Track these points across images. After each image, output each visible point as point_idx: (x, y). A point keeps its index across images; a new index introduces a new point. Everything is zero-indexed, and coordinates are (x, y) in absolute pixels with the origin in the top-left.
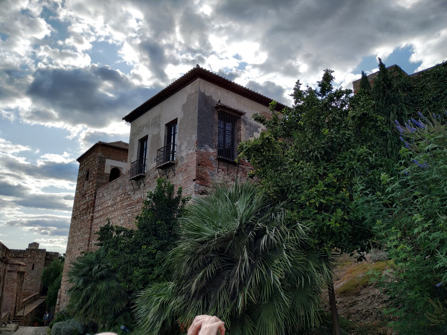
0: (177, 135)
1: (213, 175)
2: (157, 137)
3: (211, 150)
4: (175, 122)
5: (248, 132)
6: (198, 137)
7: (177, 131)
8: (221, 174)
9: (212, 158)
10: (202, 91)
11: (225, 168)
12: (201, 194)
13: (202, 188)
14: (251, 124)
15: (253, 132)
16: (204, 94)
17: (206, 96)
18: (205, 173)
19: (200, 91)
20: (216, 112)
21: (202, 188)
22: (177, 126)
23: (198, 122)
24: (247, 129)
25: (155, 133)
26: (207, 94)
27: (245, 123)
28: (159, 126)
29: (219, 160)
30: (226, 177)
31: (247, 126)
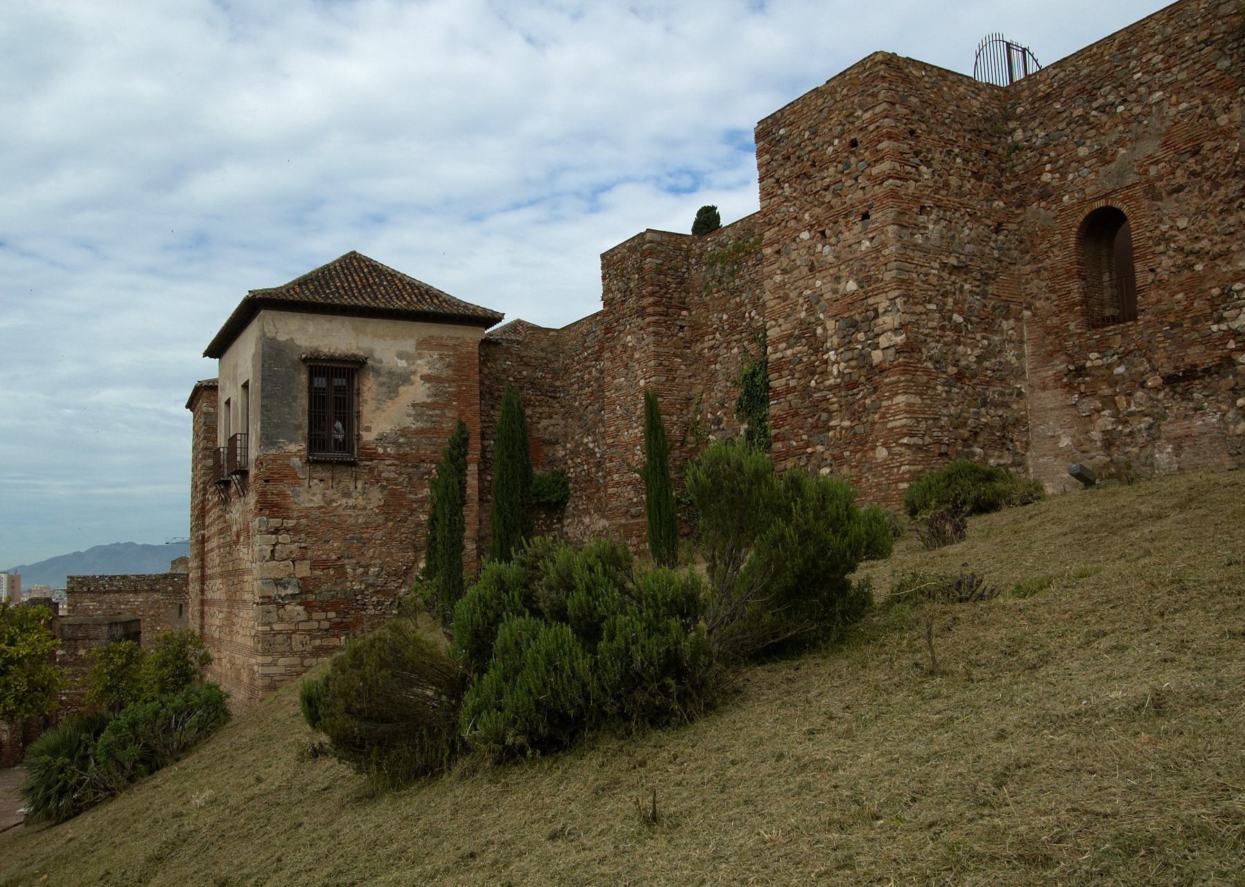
3: (293, 448)
5: (384, 389)
12: (273, 533)
13: (275, 522)
14: (391, 374)
15: (398, 386)
19: (264, 334)
21: (275, 522)
26: (282, 337)
27: (377, 372)
30: (329, 492)
31: (381, 379)
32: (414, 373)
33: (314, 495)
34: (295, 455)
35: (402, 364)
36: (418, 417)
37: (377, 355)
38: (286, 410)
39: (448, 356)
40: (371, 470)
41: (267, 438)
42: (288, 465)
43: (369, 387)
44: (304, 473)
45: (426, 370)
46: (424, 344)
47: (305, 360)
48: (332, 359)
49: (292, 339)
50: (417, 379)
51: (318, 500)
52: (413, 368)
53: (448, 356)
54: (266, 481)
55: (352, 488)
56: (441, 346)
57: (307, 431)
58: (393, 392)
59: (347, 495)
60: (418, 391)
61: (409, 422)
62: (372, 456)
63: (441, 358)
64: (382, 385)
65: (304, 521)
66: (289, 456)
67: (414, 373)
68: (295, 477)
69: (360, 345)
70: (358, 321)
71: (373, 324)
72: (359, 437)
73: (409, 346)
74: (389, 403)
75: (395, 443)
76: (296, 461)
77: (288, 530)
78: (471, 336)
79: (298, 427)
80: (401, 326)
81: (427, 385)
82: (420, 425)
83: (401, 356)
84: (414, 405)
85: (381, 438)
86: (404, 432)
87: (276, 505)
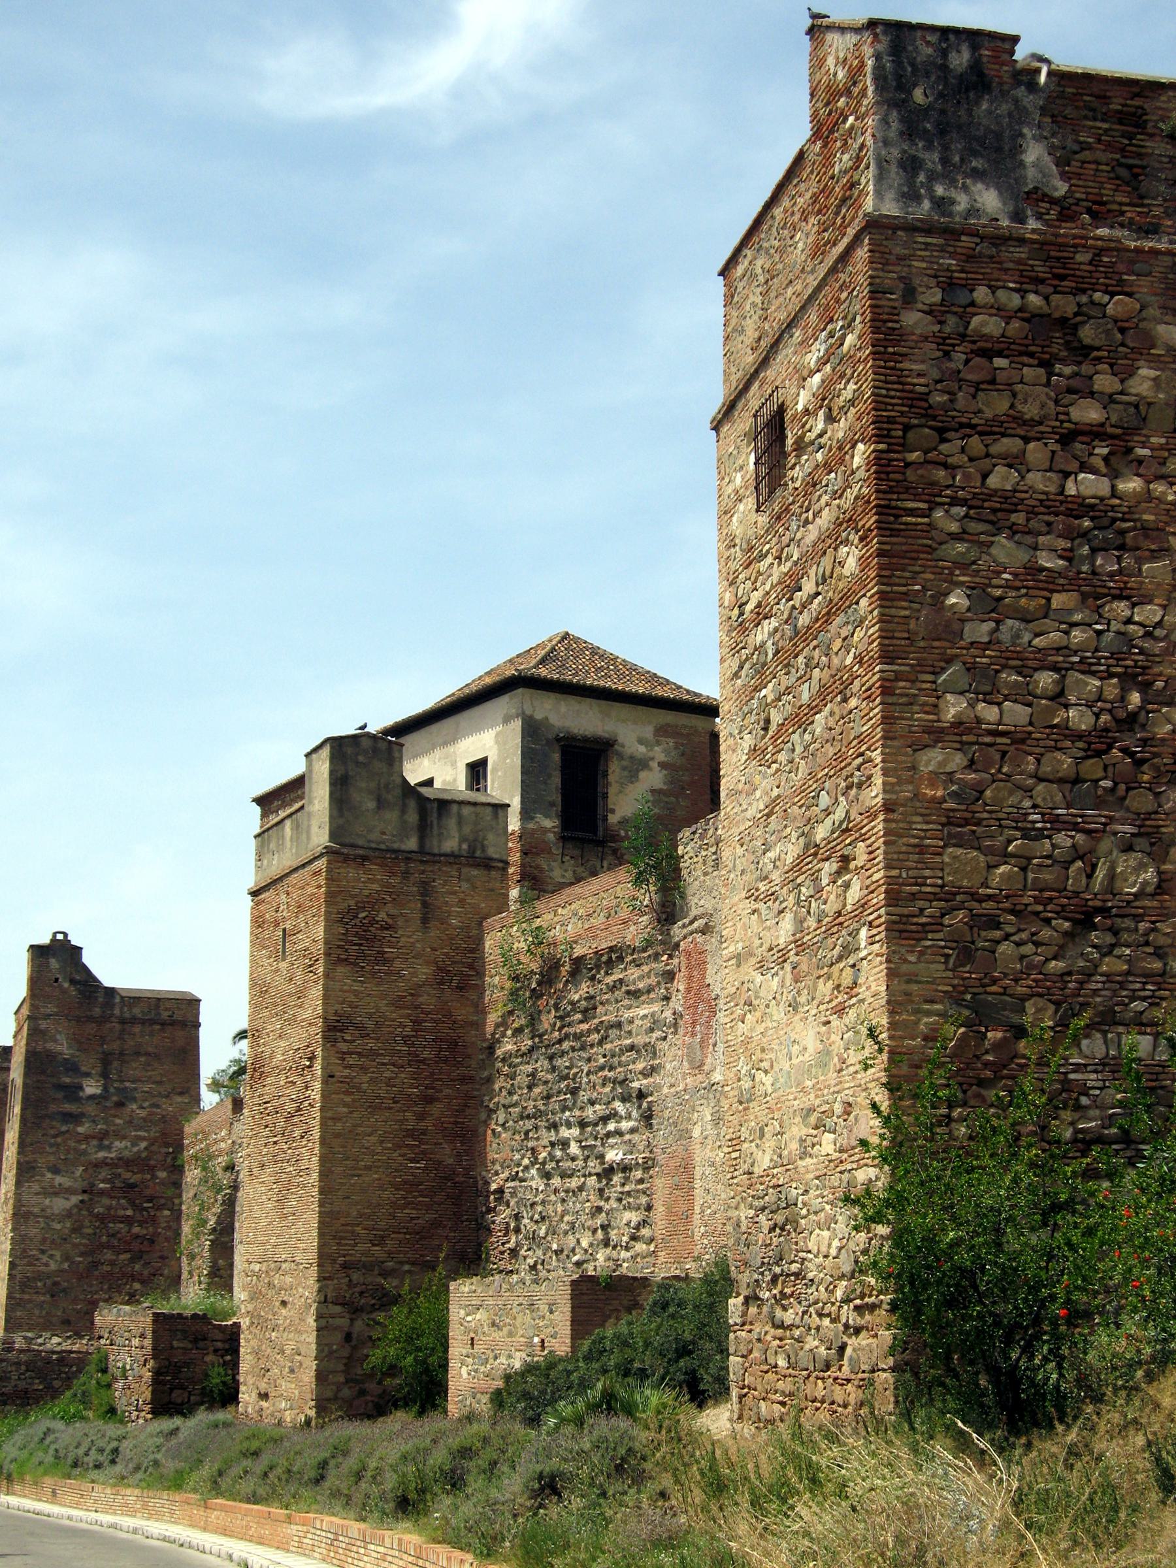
3: (548, 823)
4: (483, 762)
5: (626, 773)
6: (522, 802)
9: (551, 836)
10: (528, 712)
11: (577, 852)
14: (632, 757)
15: (638, 771)
16: (531, 717)
17: (536, 721)
18: (538, 867)
19: (523, 713)
20: (557, 748)
26: (539, 716)
27: (621, 756)
29: (564, 839)
31: (624, 763)
32: (652, 759)
33: (566, 871)
34: (549, 830)
35: (642, 749)
37: (621, 739)
38: (542, 787)
39: (682, 745)
41: (526, 812)
42: (544, 841)
43: (615, 770)
44: (558, 849)
45: (662, 757)
46: (662, 731)
47: (558, 739)
49: (547, 718)
50: (654, 764)
52: (651, 754)
53: (682, 745)
54: (525, 854)
55: (599, 867)
57: (560, 809)
60: (653, 778)
62: (615, 838)
64: (624, 768)
66: (545, 831)
67: (652, 759)
68: (550, 852)
69: (606, 728)
72: (605, 819)
73: (648, 732)
76: (551, 836)
79: (552, 804)
80: (641, 710)
81: (664, 772)
82: (656, 810)
83: (641, 741)
84: (653, 791)
85: (624, 822)
87: (534, 878)
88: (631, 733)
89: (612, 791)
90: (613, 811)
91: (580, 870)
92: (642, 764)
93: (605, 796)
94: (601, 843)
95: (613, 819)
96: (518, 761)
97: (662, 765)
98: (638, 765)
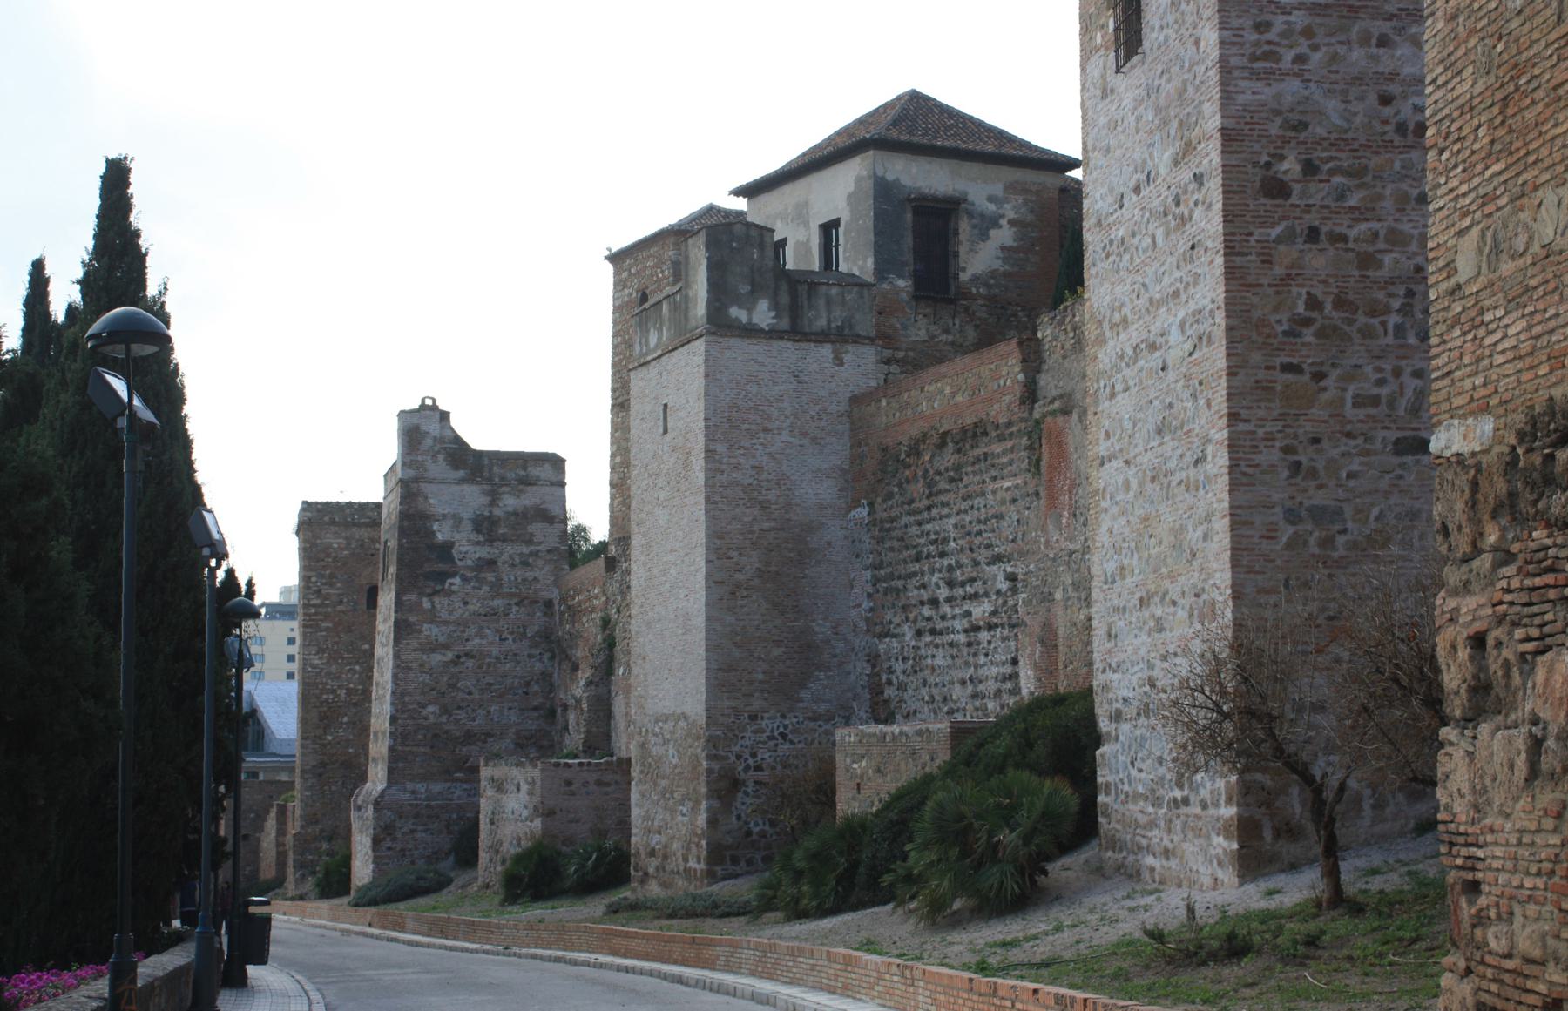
0: (841, 249)
1: (905, 328)
2: (804, 246)
3: (901, 283)
5: (976, 231)
6: (876, 263)
7: (841, 241)
8: (922, 322)
9: (904, 296)
10: (880, 174)
13: (887, 353)
14: (982, 216)
15: (988, 229)
16: (883, 178)
21: (887, 353)
22: (841, 230)
23: (876, 235)
24: (974, 227)
25: (802, 238)
26: (890, 177)
27: (971, 215)
28: (806, 224)
29: (916, 298)
31: (975, 221)
32: (1002, 216)
35: (992, 207)
36: (1005, 260)
37: (971, 198)
40: (967, 309)
45: (1011, 215)
46: (1011, 188)
48: (935, 199)
50: (1004, 222)
51: (922, 335)
56: (1025, 191)
58: (984, 236)
59: (947, 331)
60: (1004, 235)
61: (997, 264)
62: (966, 295)
63: (1026, 202)
65: (911, 354)
70: (954, 163)
71: (975, 168)
72: (956, 277)
73: (998, 189)
74: (982, 245)
75: (987, 285)
77: (898, 361)
78: (1049, 180)
80: (992, 170)
83: (991, 199)
85: (975, 279)
86: (993, 274)
88: (980, 188)
89: (963, 250)
90: (964, 269)
91: (933, 328)
92: (994, 222)
93: (956, 255)
94: (951, 301)
95: (964, 277)
96: (870, 223)
97: (1012, 223)
98: (988, 223)
